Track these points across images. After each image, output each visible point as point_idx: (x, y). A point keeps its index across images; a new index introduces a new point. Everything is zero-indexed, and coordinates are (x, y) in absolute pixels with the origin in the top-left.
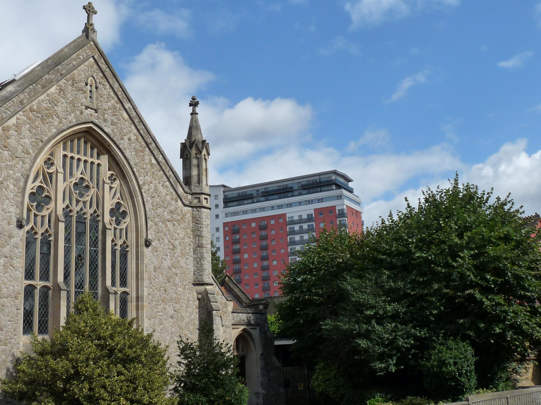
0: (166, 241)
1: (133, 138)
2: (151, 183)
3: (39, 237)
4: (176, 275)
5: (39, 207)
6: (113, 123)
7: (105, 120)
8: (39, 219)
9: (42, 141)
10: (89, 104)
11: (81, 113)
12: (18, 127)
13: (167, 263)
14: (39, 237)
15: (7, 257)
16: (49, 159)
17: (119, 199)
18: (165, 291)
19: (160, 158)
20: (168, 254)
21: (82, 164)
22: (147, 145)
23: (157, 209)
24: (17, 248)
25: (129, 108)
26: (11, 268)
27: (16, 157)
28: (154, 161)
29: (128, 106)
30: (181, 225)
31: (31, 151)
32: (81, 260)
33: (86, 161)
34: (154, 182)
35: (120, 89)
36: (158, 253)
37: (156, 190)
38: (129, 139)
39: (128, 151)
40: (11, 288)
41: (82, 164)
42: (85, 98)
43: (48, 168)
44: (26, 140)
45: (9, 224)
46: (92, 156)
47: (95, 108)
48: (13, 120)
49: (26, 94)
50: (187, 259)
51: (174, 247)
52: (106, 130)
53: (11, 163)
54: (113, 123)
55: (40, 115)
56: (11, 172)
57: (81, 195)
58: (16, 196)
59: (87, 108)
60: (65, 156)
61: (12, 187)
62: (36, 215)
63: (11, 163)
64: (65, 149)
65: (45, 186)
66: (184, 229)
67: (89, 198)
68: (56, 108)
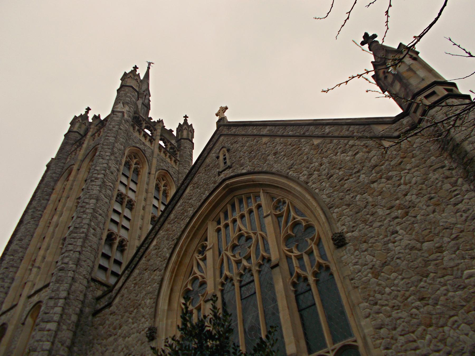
0: (380, 212)
1: (279, 148)
2: (321, 165)
4: (440, 249)
7: (242, 165)
18: (422, 299)
20: (398, 228)
23: (342, 185)
25: (269, 130)
28: (316, 142)
34: (325, 160)
36: (372, 240)
37: (332, 164)
38: (275, 154)
39: (275, 166)
50: (455, 205)
51: (407, 209)
58: (152, 307)
68: (190, 201)
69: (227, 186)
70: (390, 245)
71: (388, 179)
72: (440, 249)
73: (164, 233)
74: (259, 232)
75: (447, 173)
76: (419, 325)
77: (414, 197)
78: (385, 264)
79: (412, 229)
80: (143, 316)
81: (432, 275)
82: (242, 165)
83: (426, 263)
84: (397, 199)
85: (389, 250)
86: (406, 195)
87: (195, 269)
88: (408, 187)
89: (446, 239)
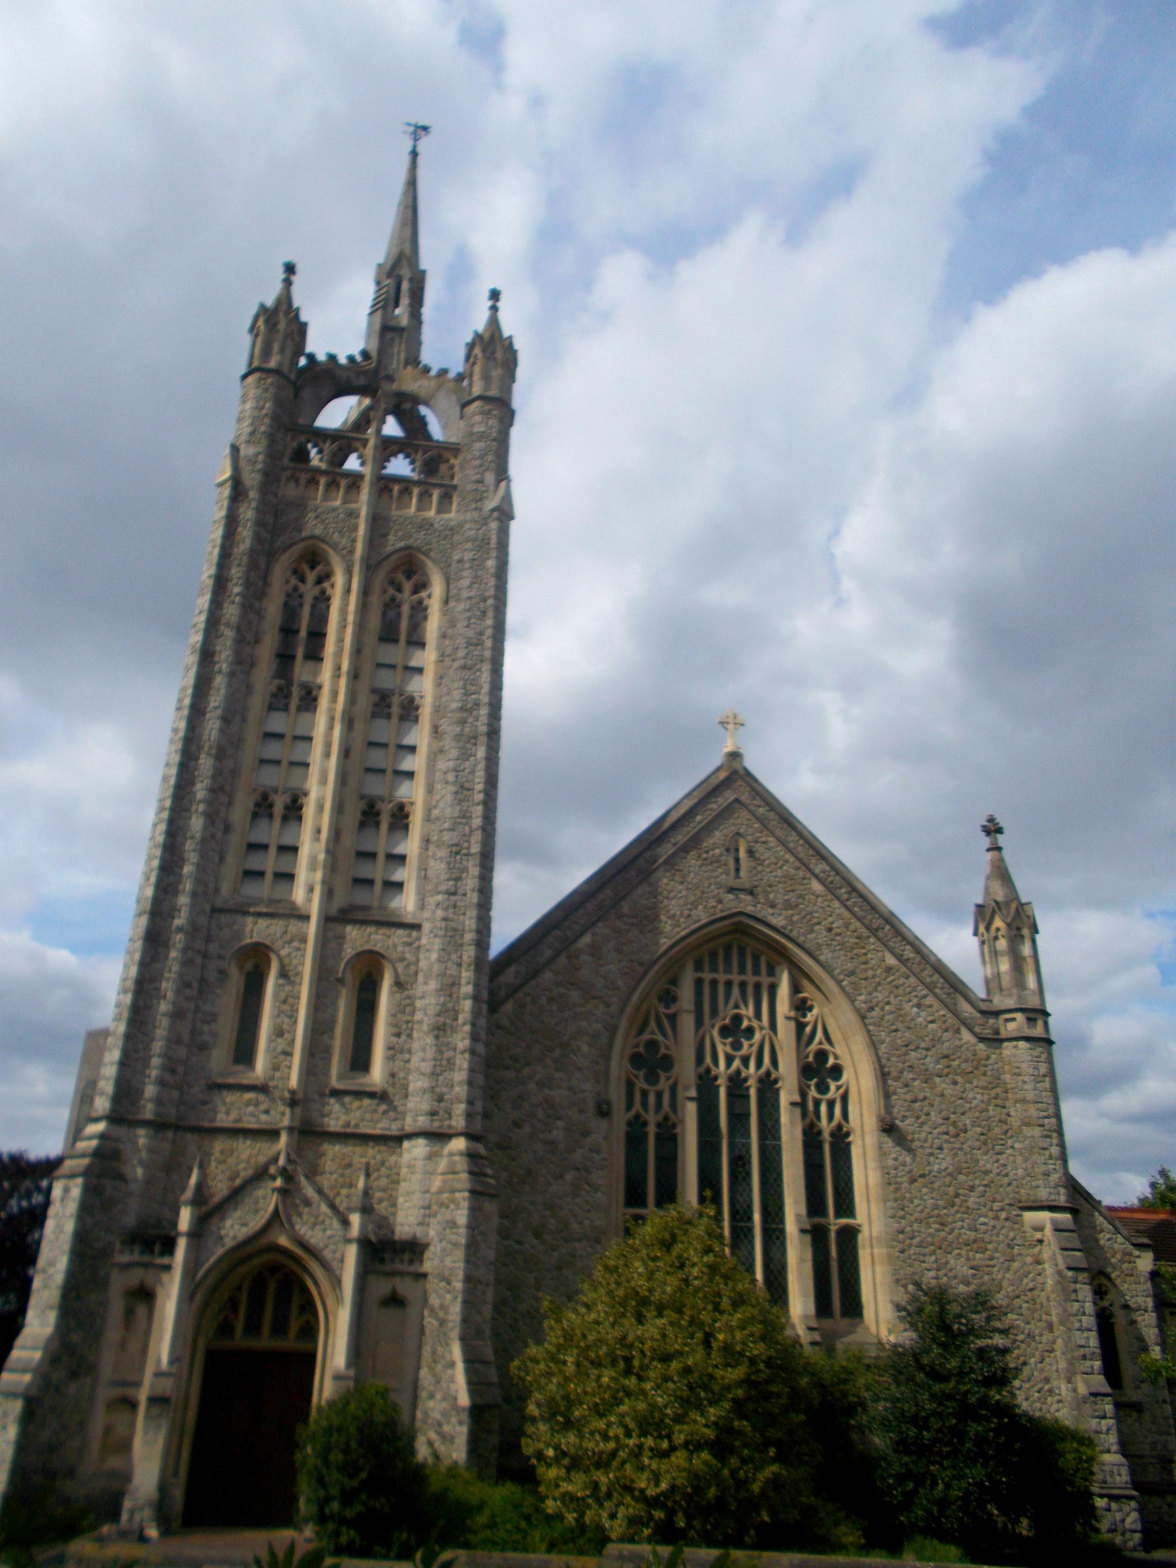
3: (652, 1129)
5: (652, 1078)
6: (788, 905)
8: (652, 1098)
9: (641, 964)
10: (731, 882)
11: (720, 901)
12: (595, 949)
13: (943, 1162)
14: (652, 1129)
15: (577, 1169)
16: (668, 992)
17: (820, 1043)
19: (908, 953)
20: (945, 1146)
21: (736, 992)
22: (874, 932)
24: (598, 1152)
26: (586, 1187)
27: (593, 998)
28: (891, 960)
29: (821, 867)
30: (975, 1084)
31: (620, 983)
32: (743, 1166)
33: (743, 985)
35: (801, 842)
40: (587, 1222)
41: (736, 992)
42: (728, 874)
43: (667, 1007)
44: (612, 967)
45: (581, 1112)
46: (756, 972)
47: (747, 886)
48: (587, 939)
49: (608, 891)
52: (774, 921)
53: (583, 1009)
54: (788, 905)
55: (634, 921)
56: (584, 1024)
57: (737, 1046)
59: (731, 890)
60: (699, 982)
61: (585, 1048)
62: (645, 1094)
63: (583, 1009)
64: (698, 967)
65: (659, 1038)
66: (983, 1088)
67: (755, 1049)
69: (740, 923)
70: (932, 1159)
71: (955, 1083)
72: (972, 1189)
73: (607, 931)
74: (767, 1031)
75: (1004, 1117)
76: (932, 1244)
77: (968, 1122)
78: (923, 1176)
79: (955, 1155)
80: (580, 1069)
81: (956, 1208)
82: (773, 906)
83: (957, 1195)
84: (954, 1113)
85: (929, 1164)
86: (963, 1114)
87: (653, 1023)
88: (967, 1105)
89: (977, 1182)
